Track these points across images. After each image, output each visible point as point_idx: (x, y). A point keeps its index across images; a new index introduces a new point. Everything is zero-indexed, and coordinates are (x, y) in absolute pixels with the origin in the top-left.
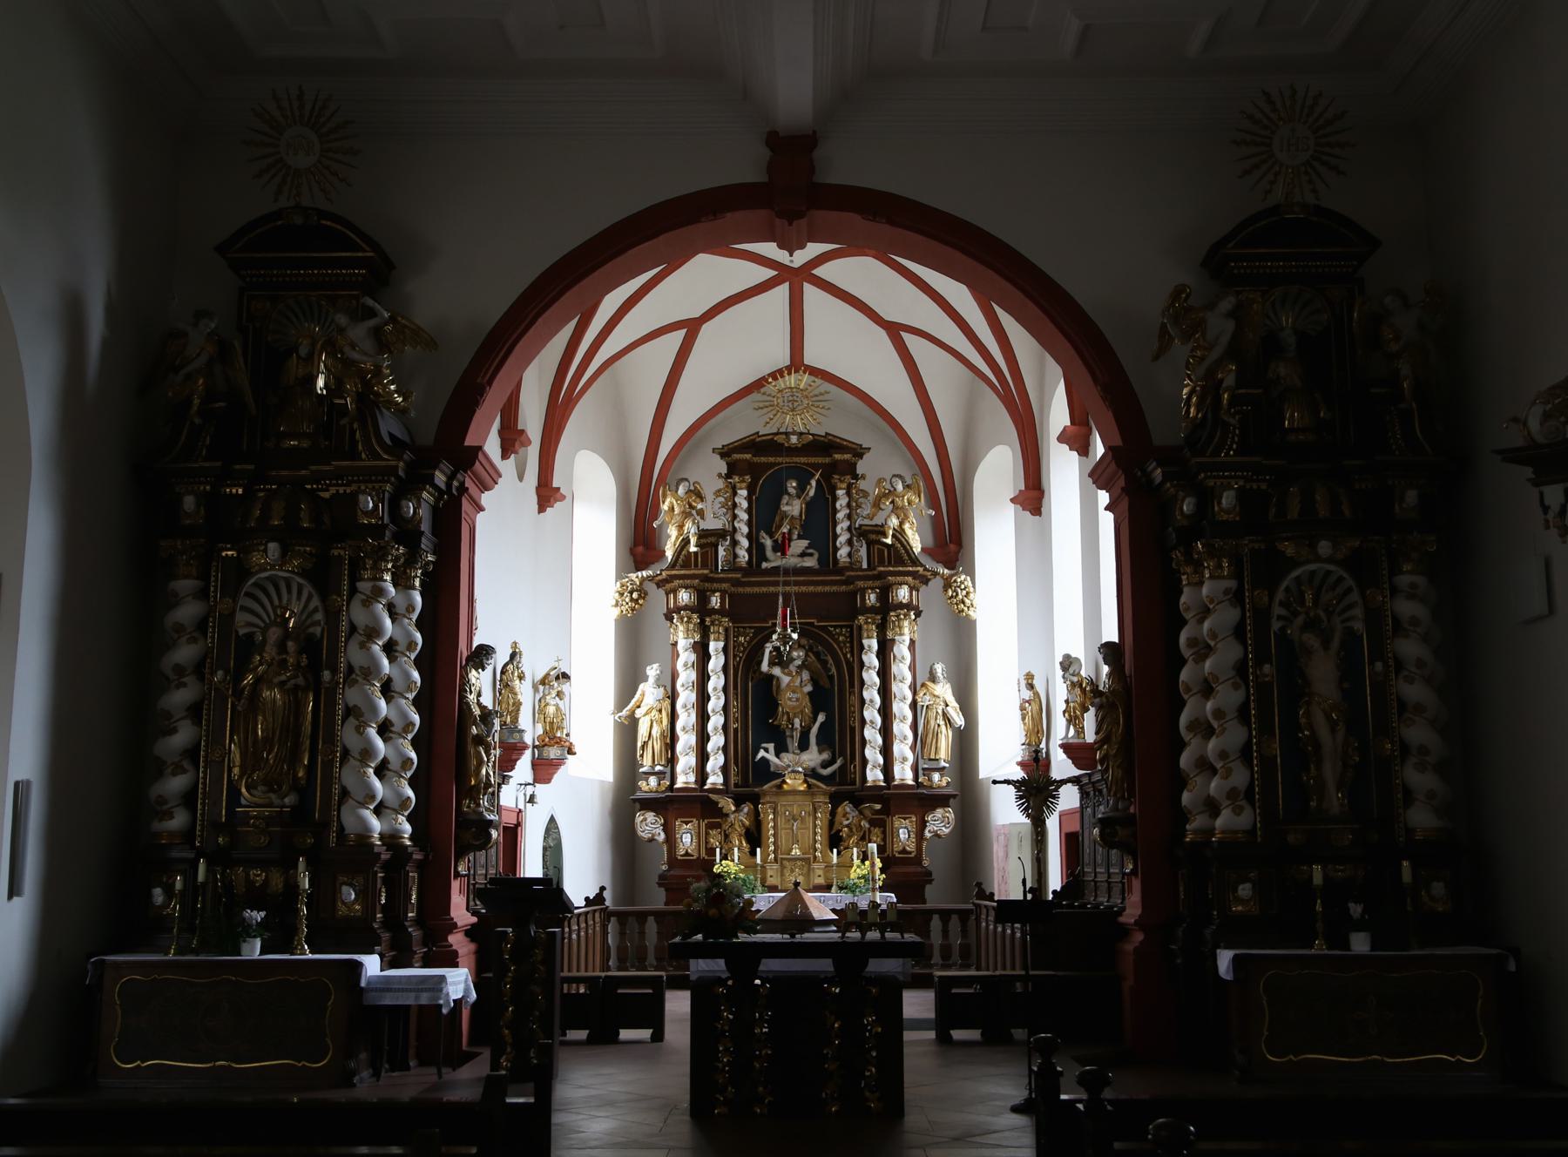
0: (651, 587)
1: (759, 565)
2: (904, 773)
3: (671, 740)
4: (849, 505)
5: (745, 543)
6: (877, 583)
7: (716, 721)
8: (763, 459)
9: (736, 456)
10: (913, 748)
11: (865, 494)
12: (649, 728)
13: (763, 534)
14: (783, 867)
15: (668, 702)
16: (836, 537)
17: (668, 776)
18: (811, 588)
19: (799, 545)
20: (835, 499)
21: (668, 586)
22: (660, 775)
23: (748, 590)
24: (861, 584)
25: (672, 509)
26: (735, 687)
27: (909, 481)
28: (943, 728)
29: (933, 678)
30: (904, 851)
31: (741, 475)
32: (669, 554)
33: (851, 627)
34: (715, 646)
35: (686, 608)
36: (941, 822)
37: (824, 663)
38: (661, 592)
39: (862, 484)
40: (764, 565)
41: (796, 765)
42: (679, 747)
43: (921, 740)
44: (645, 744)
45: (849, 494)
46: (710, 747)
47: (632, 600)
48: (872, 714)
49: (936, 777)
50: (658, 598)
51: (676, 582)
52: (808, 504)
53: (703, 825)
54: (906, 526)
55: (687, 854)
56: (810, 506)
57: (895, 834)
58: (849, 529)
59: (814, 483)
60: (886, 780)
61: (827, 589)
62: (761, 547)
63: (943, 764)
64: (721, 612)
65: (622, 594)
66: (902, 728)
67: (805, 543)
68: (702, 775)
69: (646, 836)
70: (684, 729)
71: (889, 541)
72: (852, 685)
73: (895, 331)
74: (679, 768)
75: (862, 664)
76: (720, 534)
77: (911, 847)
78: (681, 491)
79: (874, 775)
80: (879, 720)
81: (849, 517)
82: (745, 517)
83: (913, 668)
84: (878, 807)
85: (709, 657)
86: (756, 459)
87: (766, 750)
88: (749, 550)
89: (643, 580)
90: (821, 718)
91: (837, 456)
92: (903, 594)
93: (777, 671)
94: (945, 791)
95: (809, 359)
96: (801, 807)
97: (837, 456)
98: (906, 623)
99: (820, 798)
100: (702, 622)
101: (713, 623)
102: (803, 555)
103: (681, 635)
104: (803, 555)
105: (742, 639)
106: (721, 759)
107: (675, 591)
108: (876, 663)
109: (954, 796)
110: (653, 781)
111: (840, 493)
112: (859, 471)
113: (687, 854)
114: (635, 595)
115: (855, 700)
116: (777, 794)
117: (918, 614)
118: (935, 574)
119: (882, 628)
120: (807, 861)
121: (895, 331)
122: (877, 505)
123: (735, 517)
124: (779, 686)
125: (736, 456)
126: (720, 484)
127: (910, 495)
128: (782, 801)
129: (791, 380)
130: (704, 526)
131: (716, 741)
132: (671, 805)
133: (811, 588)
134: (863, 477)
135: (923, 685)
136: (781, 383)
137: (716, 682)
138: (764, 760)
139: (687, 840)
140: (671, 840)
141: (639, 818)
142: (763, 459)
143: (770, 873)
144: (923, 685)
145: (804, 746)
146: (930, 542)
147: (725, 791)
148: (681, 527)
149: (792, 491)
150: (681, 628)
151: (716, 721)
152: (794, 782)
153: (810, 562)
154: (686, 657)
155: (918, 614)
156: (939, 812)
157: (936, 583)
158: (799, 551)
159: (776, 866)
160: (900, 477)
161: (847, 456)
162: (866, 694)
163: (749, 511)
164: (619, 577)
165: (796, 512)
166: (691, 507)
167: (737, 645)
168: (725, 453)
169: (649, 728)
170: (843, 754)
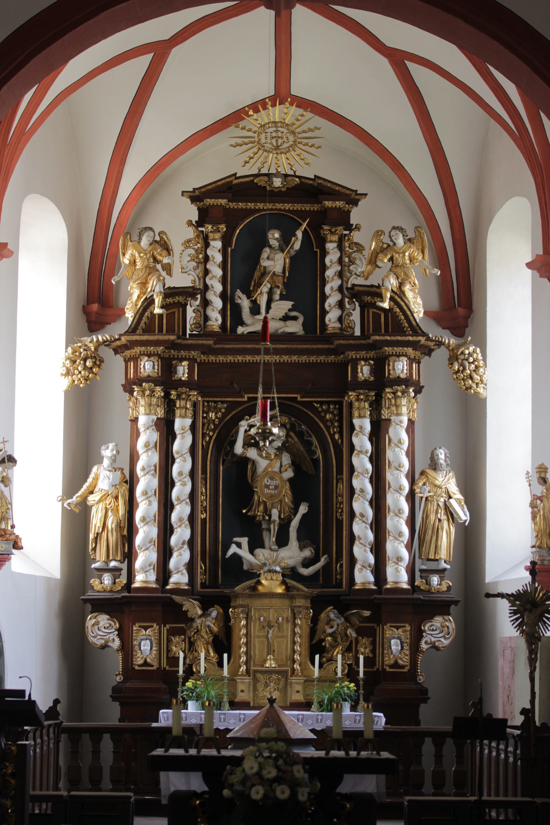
0: (107, 353)
1: (234, 329)
2: (398, 576)
3: (128, 530)
4: (340, 261)
5: (218, 303)
6: (372, 354)
7: (181, 511)
8: (241, 205)
9: (209, 201)
10: (409, 546)
11: (360, 248)
12: (103, 517)
13: (239, 293)
14: (256, 681)
15: (126, 487)
16: (324, 298)
17: (124, 573)
18: (295, 358)
19: (282, 307)
20: (324, 253)
21: (128, 353)
22: (115, 571)
23: (221, 358)
24: (352, 354)
25: (133, 263)
26: (204, 472)
27: (411, 235)
29: (434, 465)
30: (396, 665)
31: (215, 223)
32: (130, 315)
33: (341, 404)
34: (182, 424)
35: (148, 379)
36: (440, 632)
37: (308, 444)
38: (119, 360)
39: (356, 237)
40: (240, 330)
41: (275, 561)
42: (138, 540)
43: (420, 536)
44: (98, 536)
45: (340, 247)
46: (174, 540)
47: (85, 368)
48: (362, 506)
49: (435, 580)
50: (116, 365)
51: (137, 350)
52: (292, 259)
53: (164, 630)
54: (407, 288)
55: (146, 664)
56: (295, 260)
57: (386, 645)
58: (340, 289)
59: (299, 234)
60: (376, 583)
61: (313, 359)
62: (237, 310)
63: (444, 565)
64: (189, 384)
65: (74, 362)
66: (398, 523)
67: (288, 304)
68: (164, 573)
69: (99, 642)
70: (143, 519)
71: (386, 305)
72: (340, 471)
73: (398, 59)
74: (138, 564)
75: (352, 448)
76: (189, 293)
77: (405, 660)
78: (145, 242)
79: (364, 577)
80: (370, 513)
81: (340, 275)
82: (219, 272)
83: (411, 454)
84: (367, 613)
85: (174, 437)
86: (232, 205)
87: (239, 545)
88: (223, 312)
89: (99, 345)
90: (303, 509)
91: (328, 204)
92: (400, 367)
93: (252, 453)
94: (446, 597)
95: (299, 86)
96: (278, 612)
97: (328, 204)
98: (404, 401)
99: (300, 602)
100: (167, 395)
101: (179, 396)
102: (286, 318)
103: (142, 410)
104: (286, 318)
105: (212, 415)
106: (186, 555)
107: (136, 359)
108: (368, 446)
109: (456, 603)
110: (107, 579)
111: (331, 246)
112: (354, 220)
113: (146, 664)
114: (89, 363)
115: (342, 488)
116: (250, 596)
117: (418, 390)
118: (440, 344)
119: (376, 406)
120: (284, 674)
121: (398, 59)
122: (373, 261)
123: (206, 272)
124: (254, 471)
125: (209, 201)
126: (190, 233)
127: (413, 251)
128: (256, 603)
129: (276, 113)
130: (171, 282)
131: (181, 534)
132: (127, 607)
133: (295, 358)
134: (358, 228)
136: (263, 117)
137: (181, 466)
138: (237, 558)
139: (146, 648)
140: (127, 648)
141: (90, 622)
142: (241, 205)
143: (241, 687)
144: (423, 473)
145: (282, 541)
146: (435, 305)
147: (190, 592)
148: (143, 284)
149: (274, 243)
150: (142, 402)
151: (181, 511)
152: (271, 584)
153: (295, 327)
154: (147, 436)
155: (418, 390)
156: (438, 621)
157: (441, 354)
158: (282, 314)
159: (247, 679)
160: (401, 229)
161: (339, 204)
162: (356, 483)
163: (224, 266)
164: (69, 342)
165: (278, 269)
166: (155, 260)
167: (207, 422)
168: (196, 196)
169: (103, 517)
170: (327, 551)
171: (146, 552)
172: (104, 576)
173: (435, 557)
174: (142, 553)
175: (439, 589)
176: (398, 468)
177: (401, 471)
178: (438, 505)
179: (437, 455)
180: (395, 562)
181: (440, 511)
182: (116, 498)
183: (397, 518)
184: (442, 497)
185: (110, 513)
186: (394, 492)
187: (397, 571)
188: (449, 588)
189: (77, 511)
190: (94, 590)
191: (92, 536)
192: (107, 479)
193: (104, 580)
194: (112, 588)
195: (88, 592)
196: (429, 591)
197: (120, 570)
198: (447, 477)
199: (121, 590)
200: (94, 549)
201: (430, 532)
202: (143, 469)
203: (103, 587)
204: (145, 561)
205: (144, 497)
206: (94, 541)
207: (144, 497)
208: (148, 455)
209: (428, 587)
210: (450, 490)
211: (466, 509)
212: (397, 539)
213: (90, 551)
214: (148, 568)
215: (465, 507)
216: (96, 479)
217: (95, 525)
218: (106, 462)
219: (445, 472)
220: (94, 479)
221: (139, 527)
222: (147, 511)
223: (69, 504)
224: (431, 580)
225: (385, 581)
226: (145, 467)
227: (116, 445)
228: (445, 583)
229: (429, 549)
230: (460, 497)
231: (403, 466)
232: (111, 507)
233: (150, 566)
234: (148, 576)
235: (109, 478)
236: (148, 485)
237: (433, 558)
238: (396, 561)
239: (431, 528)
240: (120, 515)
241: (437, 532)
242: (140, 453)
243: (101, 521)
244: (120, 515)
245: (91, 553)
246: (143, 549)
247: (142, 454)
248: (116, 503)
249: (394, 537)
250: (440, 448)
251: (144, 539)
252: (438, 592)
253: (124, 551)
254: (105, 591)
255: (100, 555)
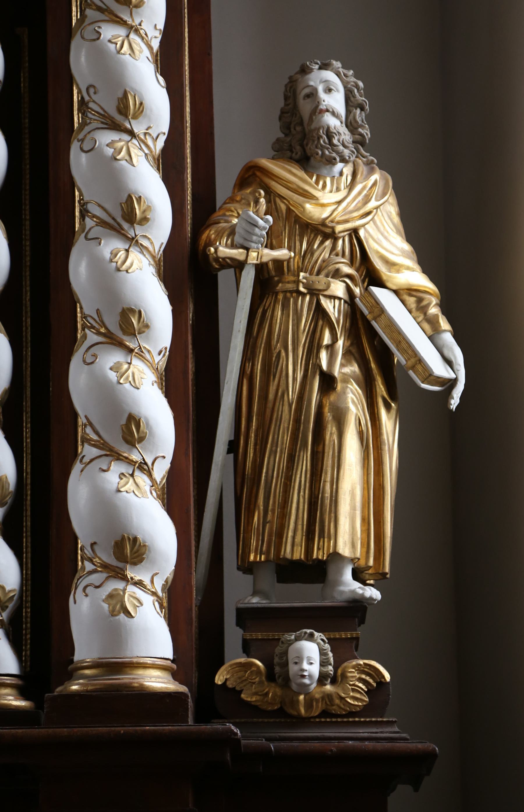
10: (181, 496)
28: (353, 398)
29: (301, 141)
43: (237, 453)
49: (310, 654)
109: (412, 767)
135: (251, 177)
173: (309, 550)
175: (328, 697)
176: (118, 118)
177: (132, 134)
178: (320, 312)
179: (313, 95)
180: (105, 567)
181: (327, 339)
183: (115, 357)
184: (337, 274)
186: (97, 231)
187: (119, 607)
188: (378, 690)
196: (284, 715)
198: (358, 188)
201: (285, 439)
209: (273, 691)
210: (373, 247)
211: (448, 338)
212: (118, 457)
215: (444, 324)
219: (348, 170)
224: (291, 655)
225: (68, 668)
228: (360, 669)
229: (284, 515)
230: (419, 279)
231: (141, 109)
237: (299, 554)
238: (112, 561)
239: (286, 415)
241: (316, 439)
249: (102, 445)
250: (324, 66)
252: (325, 713)
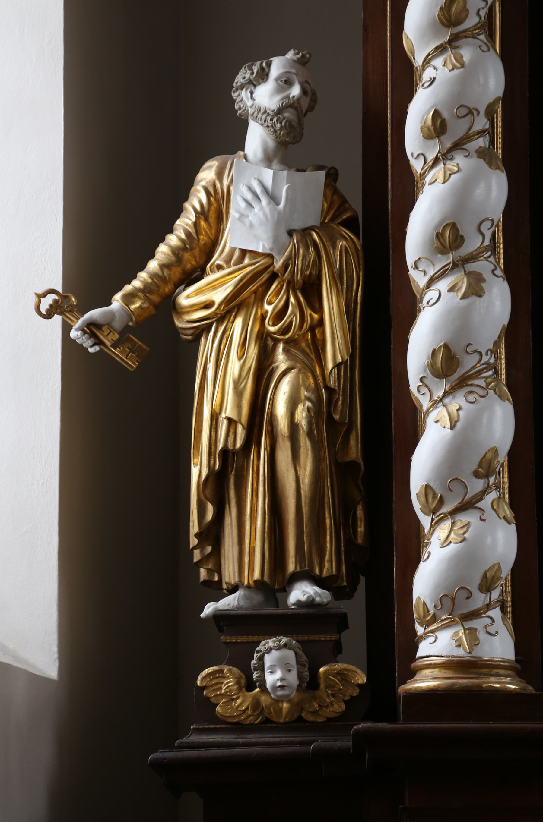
3: (370, 419)
17: (356, 636)
44: (229, 467)
70: (446, 363)
110: (276, 666)
171: (463, 518)
172: (261, 647)
174: (446, 525)
182: (310, 290)
185: (281, 361)
189: (132, 364)
190: (216, 719)
191: (198, 471)
192: (264, 201)
193: (261, 667)
194: (298, 705)
195: (186, 733)
197: (341, 622)
199: (342, 717)
200: (213, 534)
202: (437, 127)
203: (256, 704)
204: (461, 563)
205: (449, 259)
206: (209, 492)
207: (449, 259)
208: (459, 59)
213: (194, 541)
214: (480, 599)
216: (216, 213)
217: (215, 417)
218: (257, 138)
220: (202, 214)
221: (425, 402)
222: (460, 324)
223: (92, 329)
226: (445, 114)
227: (302, 62)
232: (285, 330)
233: (486, 585)
234: (482, 635)
235: (273, 198)
236: (461, 199)
240: (330, 365)
242: (418, 60)
243: (239, 394)
244: (330, 365)
245: (197, 556)
246: (446, 509)
247: (427, 61)
248: (308, 312)
251: (454, 454)
253: (350, 542)
254: (267, 724)
255: (243, 557)
